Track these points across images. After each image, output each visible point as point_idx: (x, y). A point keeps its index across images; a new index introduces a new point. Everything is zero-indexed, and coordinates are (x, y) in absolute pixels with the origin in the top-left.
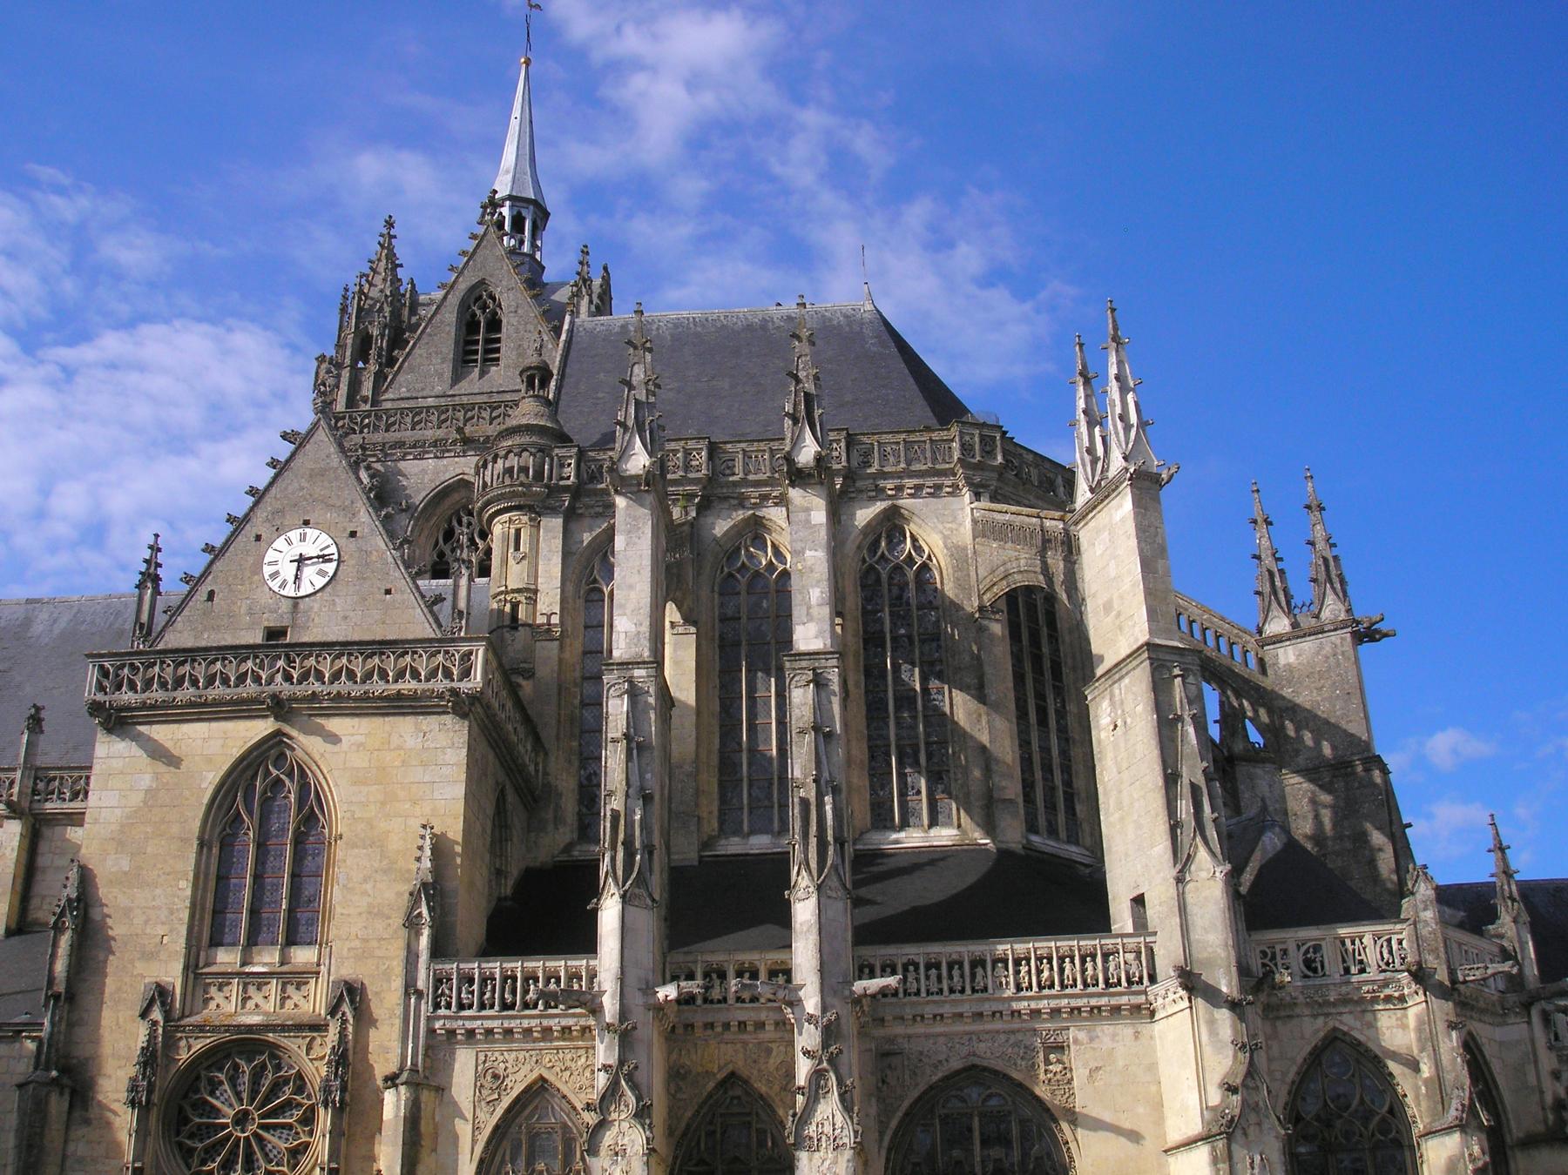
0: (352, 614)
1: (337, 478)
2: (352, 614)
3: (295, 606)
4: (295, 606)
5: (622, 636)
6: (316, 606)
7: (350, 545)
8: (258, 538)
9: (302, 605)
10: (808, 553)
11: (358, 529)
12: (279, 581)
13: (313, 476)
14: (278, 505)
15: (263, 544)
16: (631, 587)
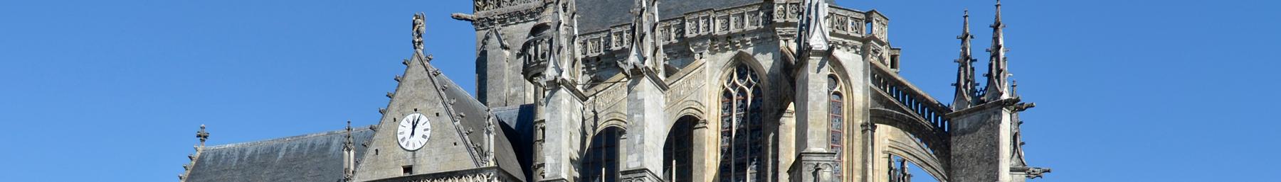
0: (439, 157)
1: (427, 85)
2: (439, 157)
3: (414, 155)
4: (414, 155)
5: (549, 165)
6: (423, 154)
7: (437, 121)
8: (395, 119)
9: (417, 154)
10: (635, 116)
11: (439, 112)
12: (405, 142)
13: (417, 84)
14: (401, 101)
15: (397, 123)
16: (552, 140)
